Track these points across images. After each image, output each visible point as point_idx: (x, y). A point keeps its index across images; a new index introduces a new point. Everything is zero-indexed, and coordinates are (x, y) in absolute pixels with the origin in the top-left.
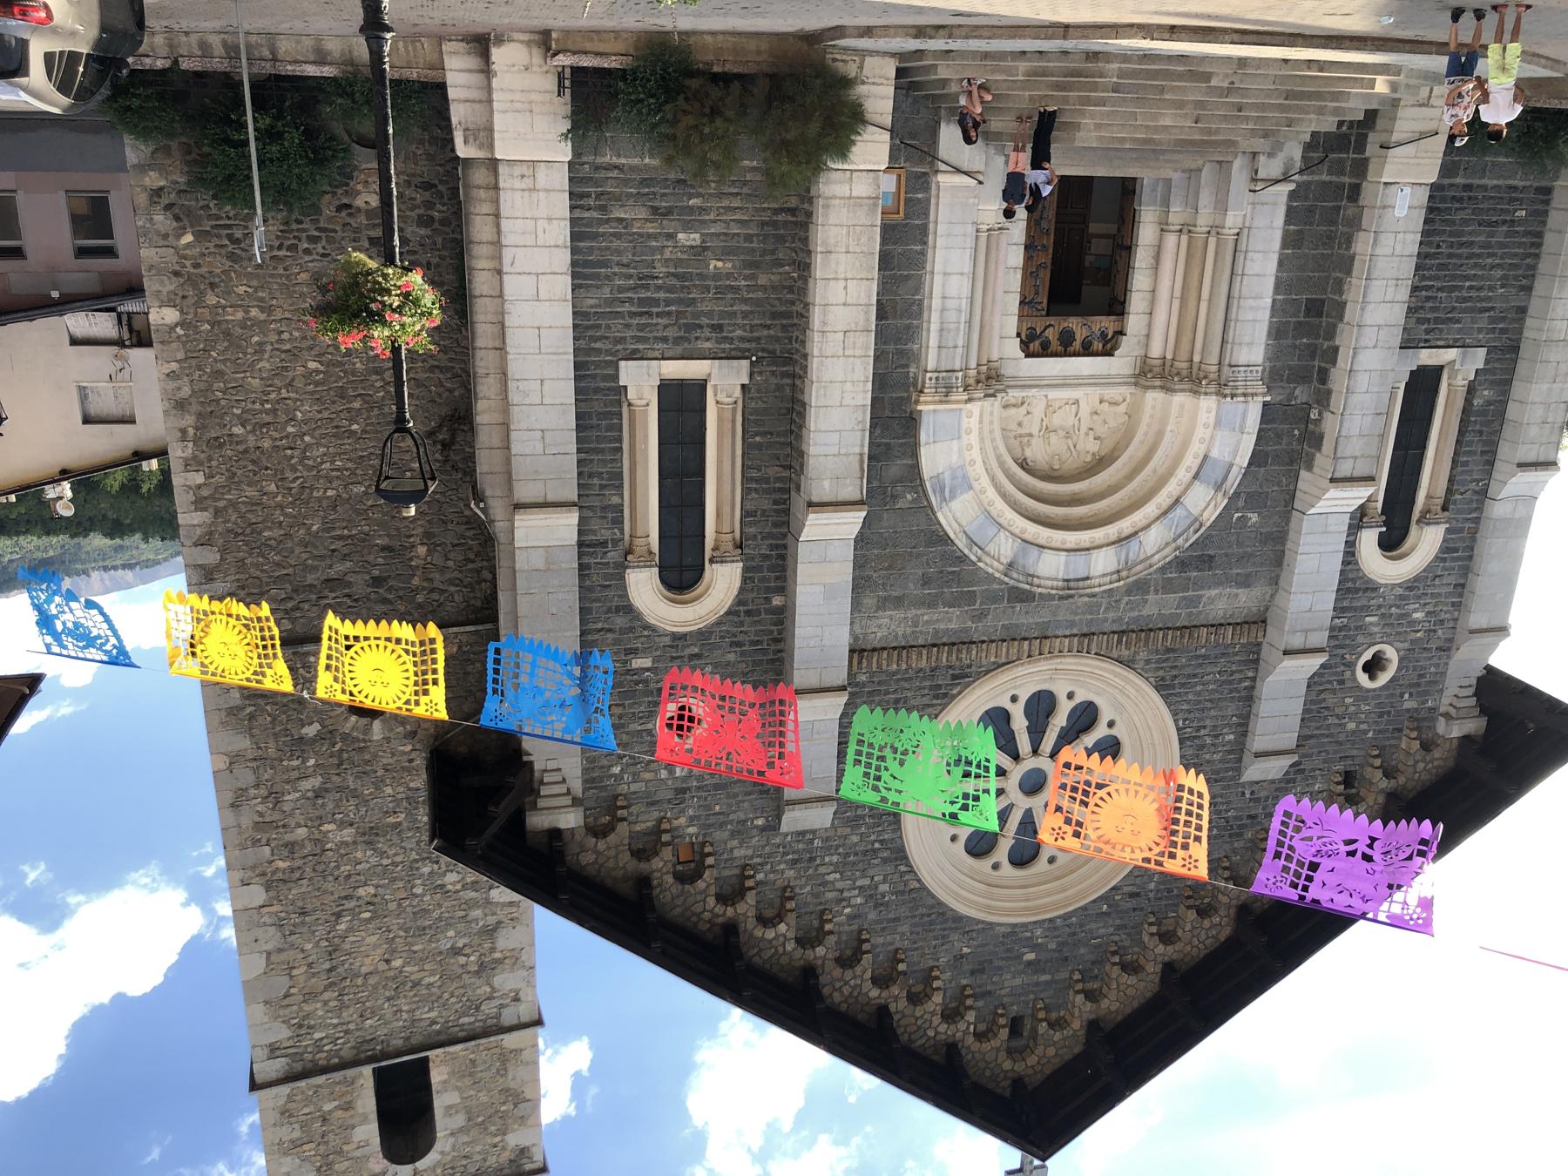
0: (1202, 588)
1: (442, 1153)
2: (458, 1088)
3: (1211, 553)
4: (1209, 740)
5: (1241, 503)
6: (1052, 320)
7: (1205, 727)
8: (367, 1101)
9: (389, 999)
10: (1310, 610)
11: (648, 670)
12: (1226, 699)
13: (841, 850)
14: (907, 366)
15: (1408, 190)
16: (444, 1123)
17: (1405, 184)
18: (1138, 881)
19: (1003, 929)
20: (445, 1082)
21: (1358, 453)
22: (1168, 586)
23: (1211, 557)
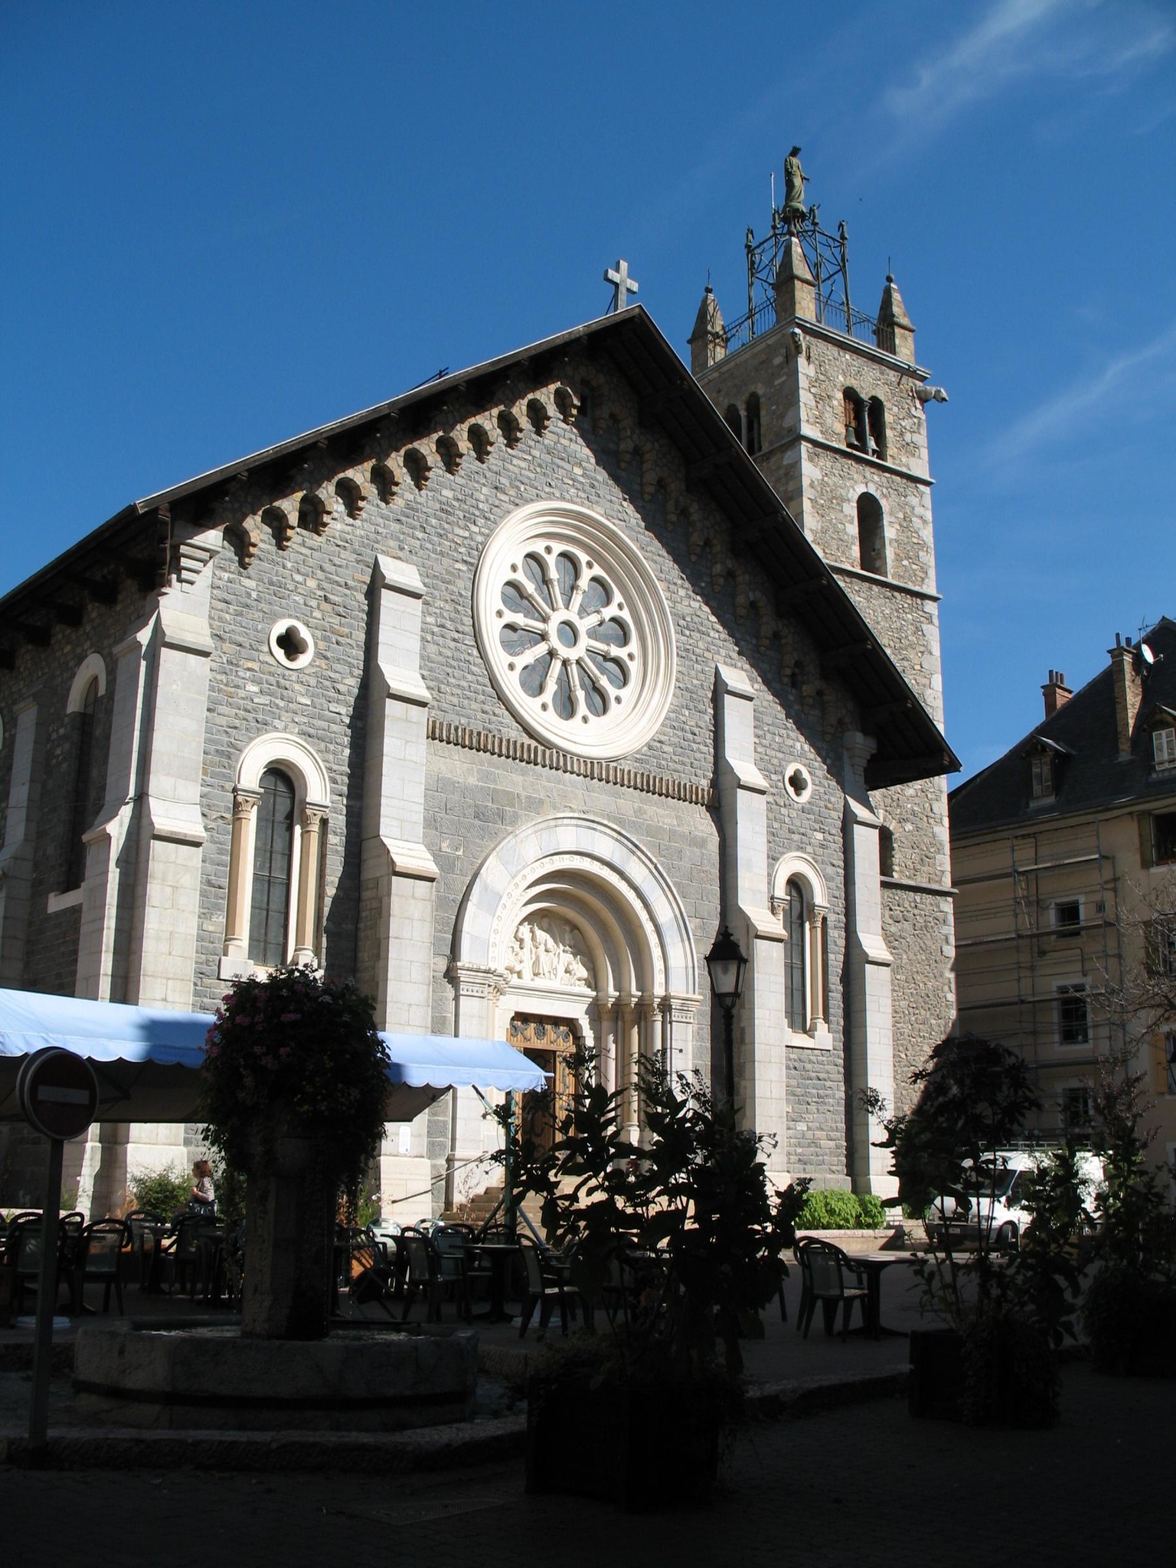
0: (482, 788)
1: (854, 490)
2: (846, 533)
3: (477, 822)
4: (448, 624)
5: (458, 864)
6: (552, 1047)
7: (454, 640)
8: (890, 553)
9: (878, 623)
10: (407, 742)
11: (815, 830)
12: (438, 663)
13: (710, 639)
14: (699, 1029)
15: (402, 1150)
16: (851, 510)
17: (405, 1156)
18: (497, 503)
19: (599, 509)
20: (852, 543)
21: (412, 902)
22: (512, 798)
23: (476, 817)
